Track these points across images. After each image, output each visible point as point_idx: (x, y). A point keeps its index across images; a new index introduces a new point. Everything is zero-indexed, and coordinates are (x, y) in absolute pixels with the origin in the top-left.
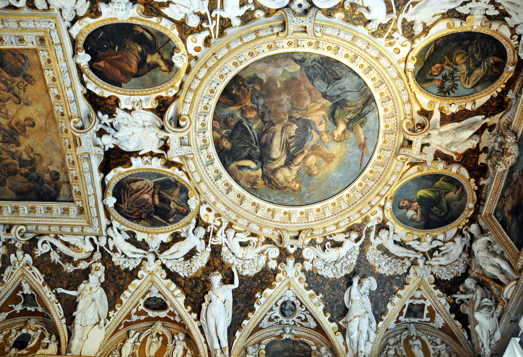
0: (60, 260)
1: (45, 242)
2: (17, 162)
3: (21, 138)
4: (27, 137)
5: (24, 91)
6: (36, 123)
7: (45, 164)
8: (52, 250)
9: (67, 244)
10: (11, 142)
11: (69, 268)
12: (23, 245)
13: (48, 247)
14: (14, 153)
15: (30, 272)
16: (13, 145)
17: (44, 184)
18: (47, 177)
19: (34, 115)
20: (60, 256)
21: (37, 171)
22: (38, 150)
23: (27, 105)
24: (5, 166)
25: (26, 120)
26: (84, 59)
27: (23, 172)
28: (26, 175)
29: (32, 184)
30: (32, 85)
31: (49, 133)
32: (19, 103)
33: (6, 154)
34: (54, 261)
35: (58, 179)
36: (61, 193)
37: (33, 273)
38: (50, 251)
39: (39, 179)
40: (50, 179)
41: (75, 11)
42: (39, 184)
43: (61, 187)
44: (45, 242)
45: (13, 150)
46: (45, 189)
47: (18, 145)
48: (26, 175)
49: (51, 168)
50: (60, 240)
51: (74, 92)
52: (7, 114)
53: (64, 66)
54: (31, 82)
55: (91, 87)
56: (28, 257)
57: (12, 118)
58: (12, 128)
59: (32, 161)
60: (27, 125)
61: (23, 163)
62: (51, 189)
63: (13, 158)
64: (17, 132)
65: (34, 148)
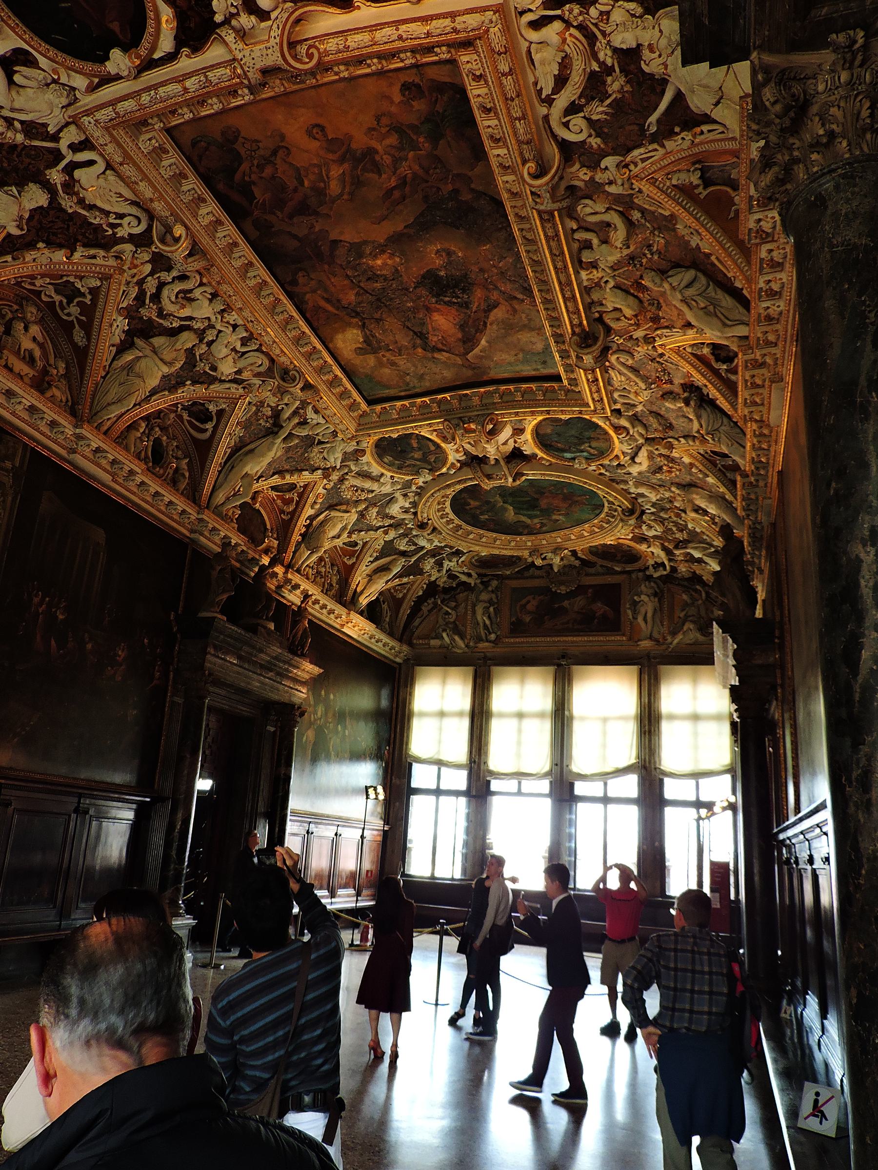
0: (602, 101)
1: (566, 125)
6: (314, 122)
7: (393, 109)
8: (582, 114)
9: (561, 81)
11: (616, 86)
12: (583, 166)
13: (577, 121)
15: (640, 165)
18: (419, 105)
20: (593, 99)
22: (368, 120)
23: (283, 137)
26: (118, 61)
30: (239, 132)
34: (606, 114)
36: (448, 80)
37: (643, 160)
38: (584, 117)
41: (48, 85)
43: (433, 80)
44: (566, 125)
45: (387, 159)
49: (397, 98)
50: (553, 94)
51: (189, 75)
53: (148, 98)
55: (166, 45)
56: (609, 162)
62: (445, 98)
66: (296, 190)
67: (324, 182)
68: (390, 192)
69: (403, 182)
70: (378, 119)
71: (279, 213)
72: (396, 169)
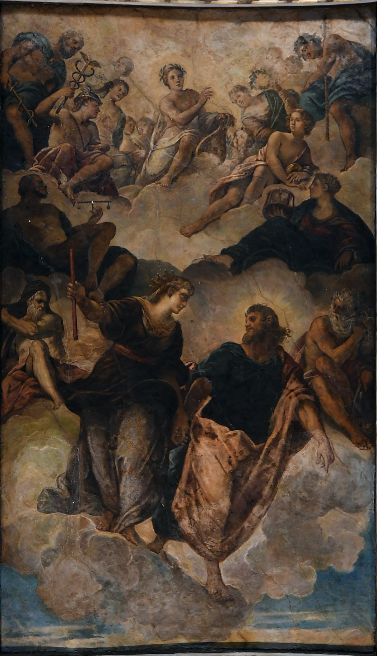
2: (276, 134)
3: (213, 107)
4: (209, 94)
5: (97, 64)
6: (174, 61)
7: (278, 67)
10: (222, 136)
14: (251, 134)
16: (230, 133)
17: (329, 79)
19: (154, 59)
21: (298, 90)
22: (241, 75)
23: (127, 72)
24: (284, 166)
25: (167, 84)
27: (298, 124)
28: (310, 121)
29: (332, 109)
30: (82, 43)
31: (200, 39)
32: (127, 87)
33: (253, 158)
35: (316, 41)
39: (320, 89)
40: (317, 60)
42: (330, 91)
43: (337, 37)
45: (242, 136)
46: (344, 79)
47: (229, 120)
48: (310, 121)
49: (288, 52)
52: (153, 124)
54: (76, 42)
57: (163, 114)
58: (186, 123)
59: (271, 94)
60: (180, 83)
61: (276, 120)
62: (344, 61)
63: (265, 142)
64: (198, 113)
65: (235, 83)
66: (104, 150)
67: (147, 148)
68: (226, 187)
69: (249, 175)
70: (254, 74)
71: (64, 179)
72: (246, 155)
